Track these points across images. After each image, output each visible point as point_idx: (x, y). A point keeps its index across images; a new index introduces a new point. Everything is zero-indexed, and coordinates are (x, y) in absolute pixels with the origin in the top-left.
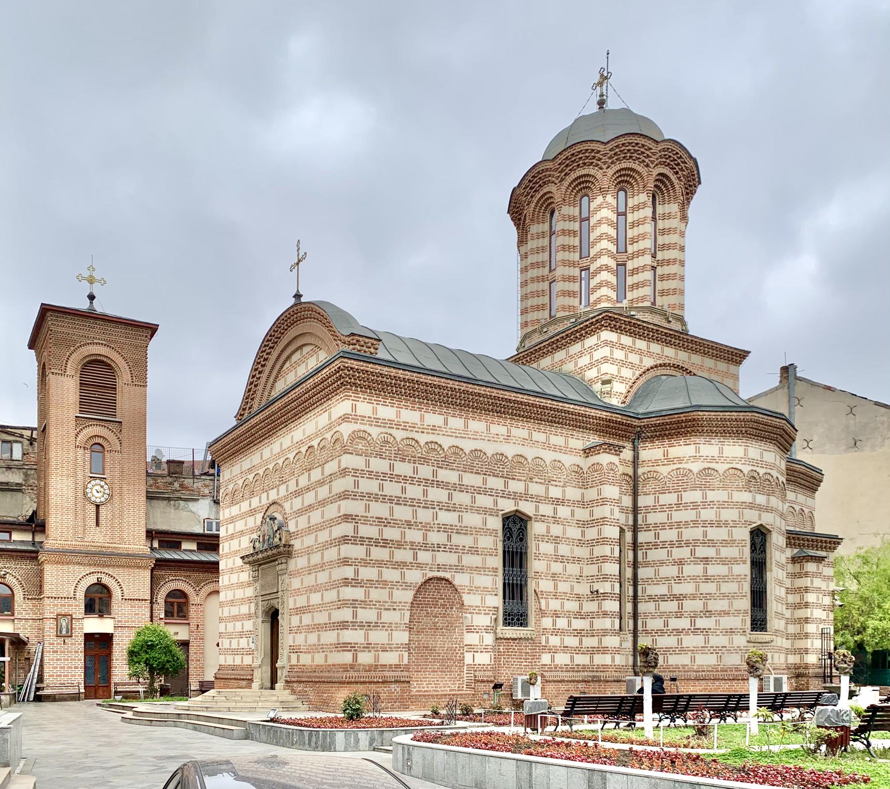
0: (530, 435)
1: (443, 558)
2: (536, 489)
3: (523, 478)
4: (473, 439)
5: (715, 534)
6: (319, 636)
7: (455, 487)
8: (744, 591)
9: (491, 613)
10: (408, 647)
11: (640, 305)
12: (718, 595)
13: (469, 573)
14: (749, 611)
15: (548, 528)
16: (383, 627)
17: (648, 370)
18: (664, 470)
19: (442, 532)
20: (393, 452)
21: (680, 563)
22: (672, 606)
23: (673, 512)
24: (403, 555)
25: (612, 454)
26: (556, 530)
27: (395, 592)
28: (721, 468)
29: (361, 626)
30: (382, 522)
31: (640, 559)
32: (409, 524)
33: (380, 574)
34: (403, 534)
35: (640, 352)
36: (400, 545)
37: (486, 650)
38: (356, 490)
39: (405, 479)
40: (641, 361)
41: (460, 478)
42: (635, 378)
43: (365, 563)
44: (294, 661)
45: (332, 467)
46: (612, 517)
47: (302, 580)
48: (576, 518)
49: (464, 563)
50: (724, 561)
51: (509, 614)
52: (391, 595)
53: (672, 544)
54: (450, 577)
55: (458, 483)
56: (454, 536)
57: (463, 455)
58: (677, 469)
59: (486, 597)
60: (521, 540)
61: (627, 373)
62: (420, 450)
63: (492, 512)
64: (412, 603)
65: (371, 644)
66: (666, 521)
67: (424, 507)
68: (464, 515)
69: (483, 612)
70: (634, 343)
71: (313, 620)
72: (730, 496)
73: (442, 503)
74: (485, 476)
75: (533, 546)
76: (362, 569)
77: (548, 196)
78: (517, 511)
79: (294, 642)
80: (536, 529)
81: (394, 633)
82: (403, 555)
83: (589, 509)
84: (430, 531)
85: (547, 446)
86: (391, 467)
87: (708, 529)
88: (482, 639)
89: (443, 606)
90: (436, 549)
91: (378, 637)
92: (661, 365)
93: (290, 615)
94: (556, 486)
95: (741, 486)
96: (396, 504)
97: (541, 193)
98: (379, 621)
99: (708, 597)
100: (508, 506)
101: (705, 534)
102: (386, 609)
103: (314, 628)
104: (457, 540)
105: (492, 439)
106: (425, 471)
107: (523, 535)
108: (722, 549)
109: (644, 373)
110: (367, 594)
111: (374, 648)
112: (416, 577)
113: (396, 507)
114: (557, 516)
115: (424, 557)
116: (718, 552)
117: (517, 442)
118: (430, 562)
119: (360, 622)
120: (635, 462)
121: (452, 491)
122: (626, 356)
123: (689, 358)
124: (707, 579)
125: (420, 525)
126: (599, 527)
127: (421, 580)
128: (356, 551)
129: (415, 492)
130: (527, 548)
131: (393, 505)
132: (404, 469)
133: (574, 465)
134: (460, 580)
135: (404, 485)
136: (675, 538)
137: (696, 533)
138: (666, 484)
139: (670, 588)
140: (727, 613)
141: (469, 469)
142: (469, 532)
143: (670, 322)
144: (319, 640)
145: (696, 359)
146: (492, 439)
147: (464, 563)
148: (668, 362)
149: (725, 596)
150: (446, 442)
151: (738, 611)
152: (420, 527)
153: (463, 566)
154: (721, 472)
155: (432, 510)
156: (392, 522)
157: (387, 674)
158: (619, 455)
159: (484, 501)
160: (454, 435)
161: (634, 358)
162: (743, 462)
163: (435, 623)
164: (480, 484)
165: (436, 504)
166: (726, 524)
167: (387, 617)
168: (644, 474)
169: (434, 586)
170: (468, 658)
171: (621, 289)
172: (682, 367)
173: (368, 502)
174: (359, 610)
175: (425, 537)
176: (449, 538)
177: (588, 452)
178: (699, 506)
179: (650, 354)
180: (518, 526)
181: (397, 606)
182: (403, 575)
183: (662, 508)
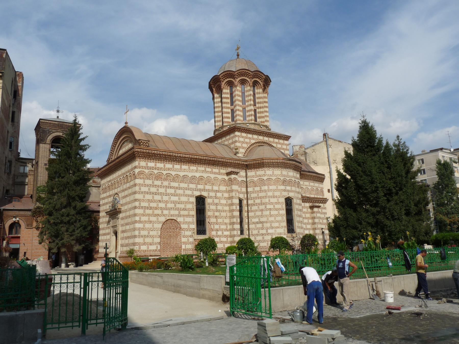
0: (205, 169)
1: (172, 212)
2: (208, 187)
5: (273, 200)
7: (177, 188)
8: (284, 219)
9: (192, 230)
10: (160, 243)
11: (251, 122)
14: (286, 226)
15: (213, 201)
17: (253, 144)
18: (255, 179)
20: (154, 177)
22: (260, 226)
24: (158, 212)
26: (216, 201)
27: (155, 225)
29: (142, 237)
30: (149, 201)
32: (160, 201)
33: (149, 219)
35: (250, 138)
36: (156, 208)
37: (190, 243)
38: (140, 191)
39: (158, 186)
40: (250, 141)
41: (179, 185)
42: (248, 147)
43: (143, 215)
45: (132, 183)
48: (224, 196)
49: (181, 214)
51: (199, 231)
52: (153, 226)
53: (259, 204)
54: (176, 219)
55: (178, 186)
59: (190, 225)
60: (203, 205)
61: (245, 145)
62: (164, 176)
63: (192, 196)
64: (161, 228)
69: (189, 230)
70: (247, 135)
75: (207, 207)
76: (142, 217)
77: (219, 86)
78: (201, 195)
80: (208, 201)
81: (154, 239)
82: (158, 212)
85: (212, 172)
86: (153, 182)
87: (271, 199)
88: (188, 240)
89: (173, 229)
90: (170, 209)
91: (148, 240)
92: (257, 142)
94: (216, 186)
97: (217, 84)
98: (149, 235)
99: (272, 222)
100: (197, 194)
101: (269, 200)
104: (178, 206)
106: (166, 183)
107: (204, 203)
108: (275, 205)
109: (251, 145)
110: (144, 226)
112: (163, 219)
113: (155, 196)
115: (166, 212)
116: (274, 206)
118: (168, 214)
120: (246, 177)
122: (244, 140)
123: (269, 139)
124: (271, 216)
129: (162, 190)
130: (205, 208)
131: (154, 195)
132: (158, 183)
134: (180, 219)
137: (267, 200)
140: (278, 227)
141: (182, 182)
143: (261, 127)
145: (271, 139)
147: (181, 214)
148: (260, 141)
149: (277, 221)
150: (173, 173)
151: (282, 227)
155: (169, 196)
157: (151, 253)
158: (237, 175)
159: (189, 192)
161: (247, 140)
163: (170, 235)
166: (276, 197)
167: (152, 233)
168: (249, 180)
169: (170, 222)
170: (183, 247)
171: (245, 117)
172: (266, 143)
173: (144, 195)
174: (141, 231)
175: (166, 205)
176: (175, 206)
179: (253, 139)
180: (202, 200)
182: (158, 219)
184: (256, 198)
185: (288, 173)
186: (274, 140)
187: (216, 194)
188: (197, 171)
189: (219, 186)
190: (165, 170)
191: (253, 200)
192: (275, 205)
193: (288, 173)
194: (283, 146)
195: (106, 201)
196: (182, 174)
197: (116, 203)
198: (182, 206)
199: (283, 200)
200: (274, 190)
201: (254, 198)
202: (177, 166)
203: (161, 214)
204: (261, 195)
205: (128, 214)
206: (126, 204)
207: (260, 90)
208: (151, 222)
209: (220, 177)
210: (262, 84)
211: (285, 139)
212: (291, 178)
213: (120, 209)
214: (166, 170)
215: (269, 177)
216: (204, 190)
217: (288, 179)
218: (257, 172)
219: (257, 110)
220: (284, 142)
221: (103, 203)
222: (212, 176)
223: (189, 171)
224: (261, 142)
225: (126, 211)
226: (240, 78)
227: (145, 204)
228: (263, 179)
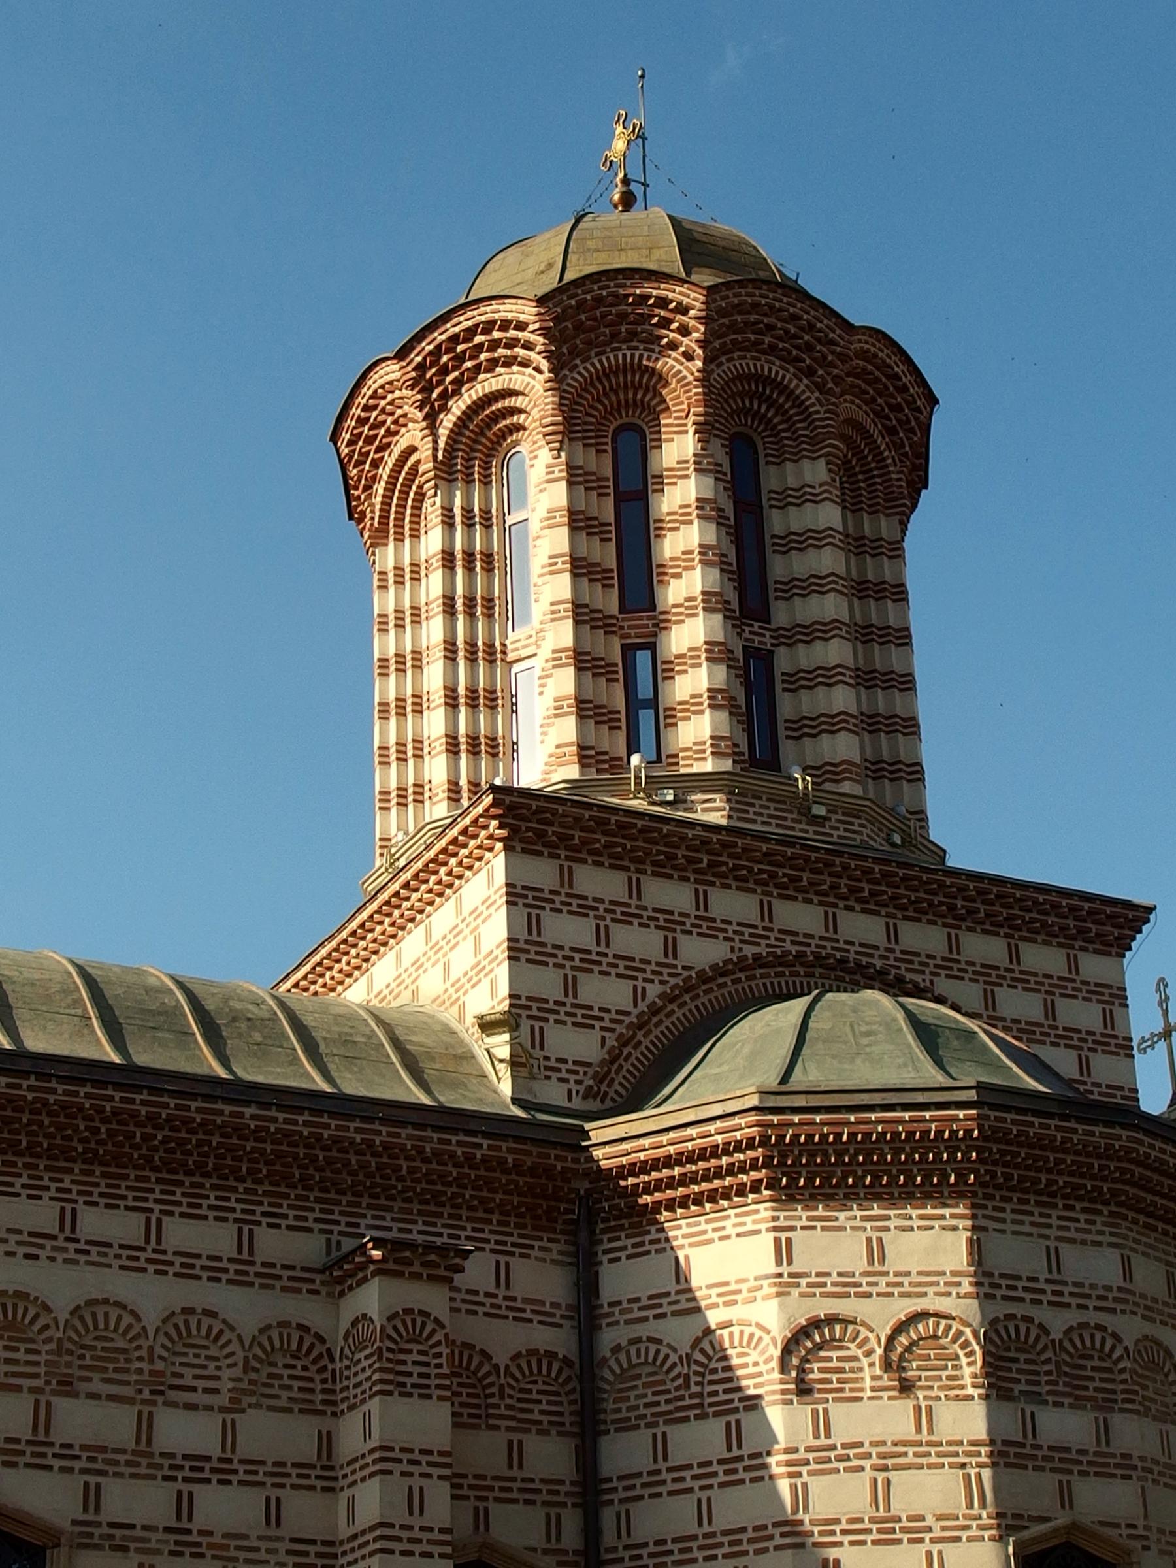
3: (26, 1383)
17: (703, 977)
25: (417, 1276)
40: (670, 948)
42: (642, 1006)
46: (416, 1522)
66: (693, 1529)
70: (635, 889)
94: (191, 1407)
97: (397, 451)
114: (194, 1527)
122: (602, 936)
123: (893, 934)
133: (283, 1324)
138: (688, 1387)
148: (794, 949)
166: (916, 1530)
168: (616, 1349)
179: (710, 928)
185: (1054, 1259)
186: (953, 944)
187: (184, 1505)
189: (235, 1407)
193: (1054, 1259)
194: (1061, 1002)
207: (806, 464)
210: (819, 412)
211: (1081, 931)
212: (1093, 1317)
215: (823, 1307)
217: (1058, 1322)
219: (783, 661)
220: (1073, 965)
224: (800, 955)
226: (597, 363)
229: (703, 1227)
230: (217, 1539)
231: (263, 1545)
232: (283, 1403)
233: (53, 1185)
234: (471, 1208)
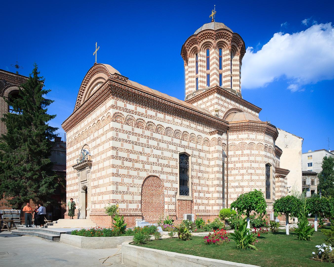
1: (155, 168)
2: (192, 145)
4: (168, 123)
6: (103, 197)
7: (160, 140)
8: (264, 185)
12: (255, 186)
13: (166, 174)
14: (265, 192)
15: (197, 160)
16: (130, 193)
18: (237, 143)
19: (155, 158)
21: (243, 175)
23: (240, 157)
26: (200, 161)
28: (256, 143)
29: (120, 193)
31: (229, 173)
33: (128, 172)
34: (138, 157)
36: (137, 161)
39: (139, 135)
43: (122, 167)
44: (93, 208)
47: (96, 174)
48: (207, 157)
50: (257, 175)
52: (133, 181)
56: (160, 160)
57: (164, 128)
58: (242, 142)
60: (186, 163)
63: (176, 152)
64: (142, 185)
65: (124, 200)
66: (238, 160)
67: (147, 147)
68: (164, 152)
71: (100, 191)
72: (259, 152)
73: (155, 146)
74: (172, 138)
78: (185, 152)
79: (93, 200)
83: (211, 154)
84: (150, 157)
90: (153, 164)
91: (127, 197)
93: (92, 189)
95: (263, 149)
96: (135, 144)
98: (128, 191)
101: (251, 165)
102: (131, 187)
103: (100, 194)
104: (161, 161)
105: (175, 124)
106: (147, 133)
108: (257, 170)
110: (123, 180)
111: (126, 202)
115: (147, 167)
116: (255, 171)
117: (185, 126)
119: (119, 191)
121: (159, 142)
125: (145, 154)
126: (215, 160)
127: (146, 176)
128: (119, 162)
129: (143, 140)
135: (139, 137)
136: (241, 166)
139: (239, 184)
142: (166, 159)
144: (102, 198)
146: (175, 124)
150: (157, 123)
152: (145, 155)
153: (163, 172)
154: (256, 144)
156: (133, 152)
160: (160, 120)
162: (263, 141)
164: (171, 141)
165: (152, 146)
167: (131, 190)
175: (148, 159)
176: (158, 160)
177: (211, 133)
178: (249, 155)
181: (136, 186)
182: (138, 174)
183: (237, 156)
184: (237, 162)
188: (181, 125)
189: (203, 145)
190: (147, 117)
191: (233, 164)
192: (257, 170)
195: (73, 155)
196: (165, 125)
197: (85, 155)
198: (165, 162)
199: (264, 166)
200: (256, 155)
201: (234, 162)
202: (161, 115)
203: (142, 168)
204: (242, 159)
205: (101, 166)
206: (98, 154)
208: (130, 176)
209: (204, 136)
213: (91, 161)
214: (148, 117)
216: (188, 147)
218: (239, 135)
221: (70, 157)
222: (197, 133)
223: (173, 123)
225: (98, 163)
227: (124, 155)
228: (246, 143)
229: (240, 133)
230: (202, 157)
231: (205, 158)
232: (206, 145)
233: (189, 121)
234: (220, 128)
